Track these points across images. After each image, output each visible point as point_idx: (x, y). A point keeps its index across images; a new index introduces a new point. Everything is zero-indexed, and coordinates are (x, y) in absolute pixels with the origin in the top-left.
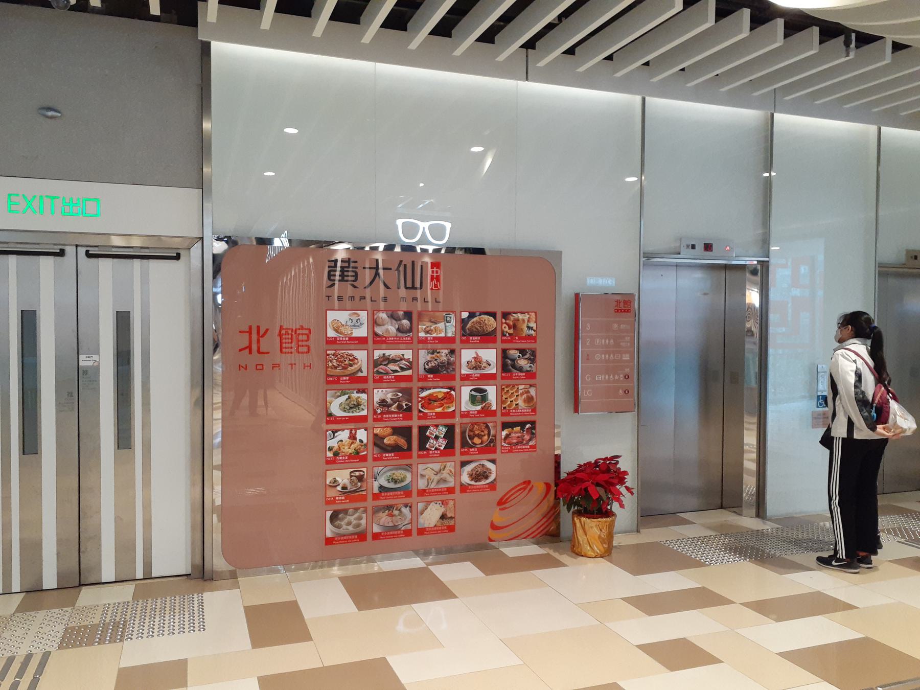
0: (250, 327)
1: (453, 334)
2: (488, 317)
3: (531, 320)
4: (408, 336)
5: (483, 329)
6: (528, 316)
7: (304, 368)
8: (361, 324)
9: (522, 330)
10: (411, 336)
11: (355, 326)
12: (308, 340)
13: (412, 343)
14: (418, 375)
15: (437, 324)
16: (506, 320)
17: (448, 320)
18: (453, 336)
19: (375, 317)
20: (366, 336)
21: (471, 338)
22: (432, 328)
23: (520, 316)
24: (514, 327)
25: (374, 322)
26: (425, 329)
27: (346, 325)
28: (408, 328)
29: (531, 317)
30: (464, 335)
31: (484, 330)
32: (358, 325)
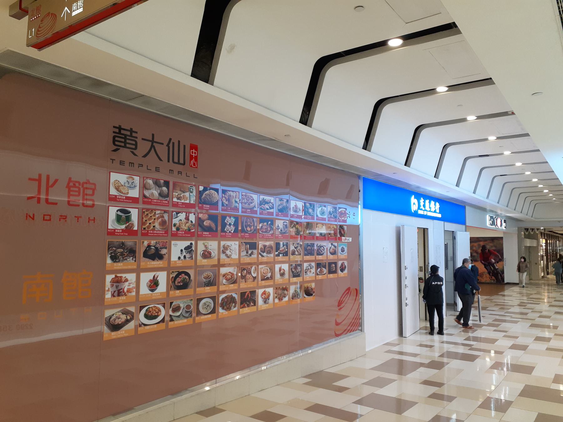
0: (40, 175)
1: (194, 202)
2: (214, 191)
3: (237, 197)
4: (166, 200)
5: (211, 200)
6: (235, 194)
7: (89, 222)
8: (135, 186)
9: (232, 202)
10: (168, 200)
11: (130, 187)
12: (93, 194)
13: (168, 206)
14: (172, 231)
15: (184, 193)
16: (224, 195)
17: (191, 190)
18: (194, 203)
19: (145, 182)
20: (138, 197)
21: (204, 206)
22: (181, 195)
23: (232, 193)
24: (228, 200)
25: (144, 187)
26: (177, 196)
27: (124, 186)
28: (166, 194)
29: (237, 195)
30: (200, 203)
31: (212, 201)
32: (132, 187)
